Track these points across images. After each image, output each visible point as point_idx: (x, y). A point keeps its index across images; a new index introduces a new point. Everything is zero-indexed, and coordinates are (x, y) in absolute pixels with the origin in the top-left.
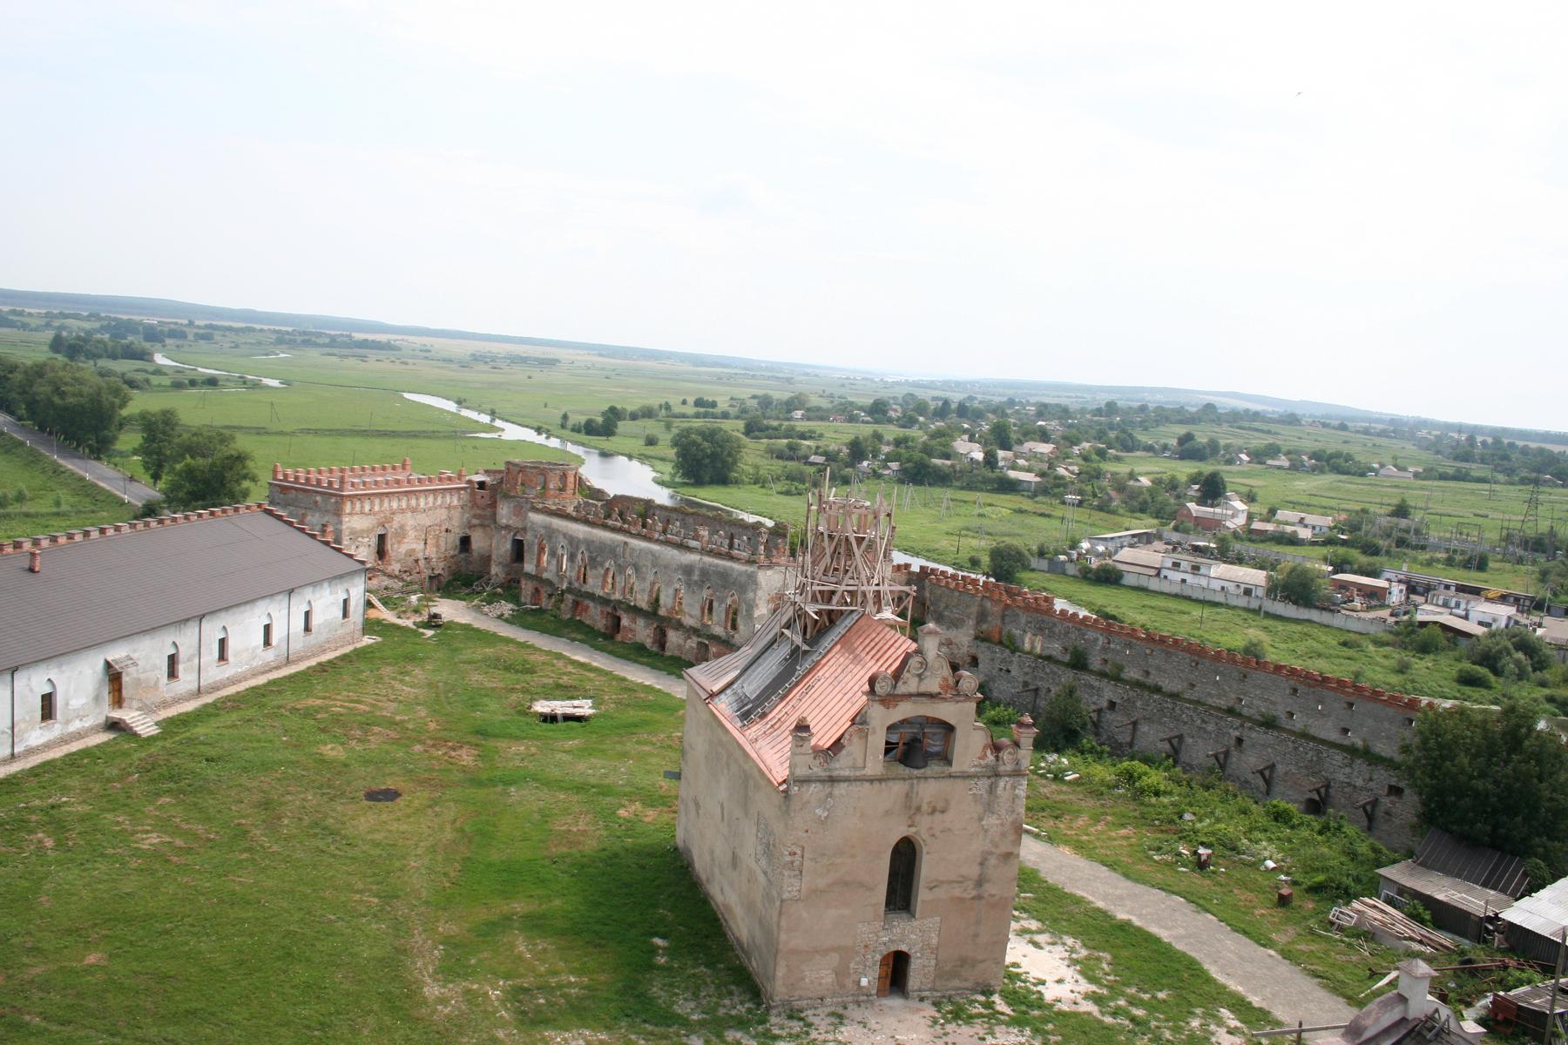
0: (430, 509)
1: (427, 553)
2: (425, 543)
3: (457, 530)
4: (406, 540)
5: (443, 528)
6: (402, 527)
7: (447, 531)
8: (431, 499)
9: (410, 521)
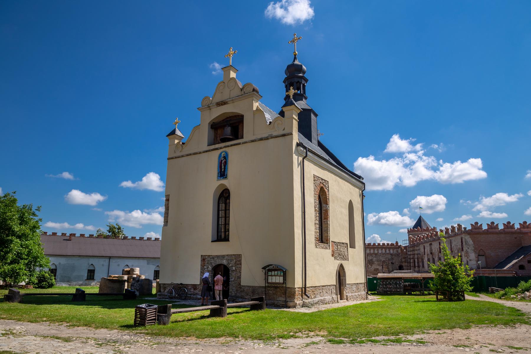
0: (383, 254)
1: (384, 271)
2: (383, 267)
3: (397, 263)
4: (373, 265)
5: (390, 262)
6: (372, 260)
7: (392, 263)
8: (384, 250)
9: (374, 259)
